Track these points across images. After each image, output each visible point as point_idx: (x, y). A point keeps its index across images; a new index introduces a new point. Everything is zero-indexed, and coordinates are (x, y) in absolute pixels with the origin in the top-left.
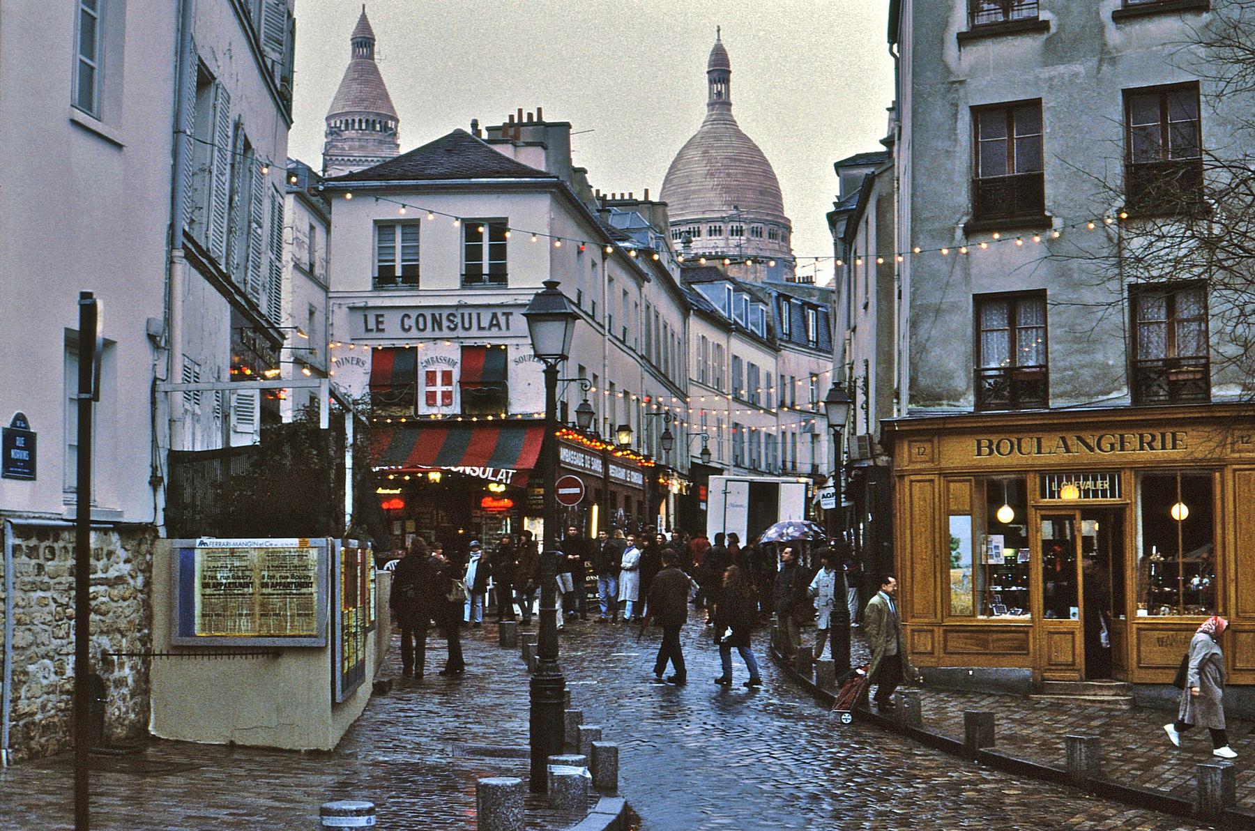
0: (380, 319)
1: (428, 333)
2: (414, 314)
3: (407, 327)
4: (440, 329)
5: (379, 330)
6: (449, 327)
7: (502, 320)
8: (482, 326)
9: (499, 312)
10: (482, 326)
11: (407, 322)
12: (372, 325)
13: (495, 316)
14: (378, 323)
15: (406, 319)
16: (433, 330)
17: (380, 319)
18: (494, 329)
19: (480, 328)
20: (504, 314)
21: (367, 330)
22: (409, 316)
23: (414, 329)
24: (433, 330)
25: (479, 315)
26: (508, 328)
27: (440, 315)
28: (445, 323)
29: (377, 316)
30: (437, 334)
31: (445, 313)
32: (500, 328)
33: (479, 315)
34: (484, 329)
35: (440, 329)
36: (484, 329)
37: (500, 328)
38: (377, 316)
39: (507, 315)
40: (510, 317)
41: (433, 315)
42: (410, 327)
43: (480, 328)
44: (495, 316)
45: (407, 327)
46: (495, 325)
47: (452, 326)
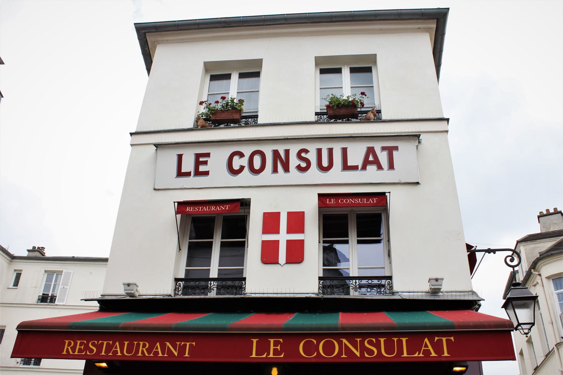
0: (201, 159)
1: (267, 176)
2: (247, 151)
3: (236, 167)
4: (286, 169)
5: (198, 173)
6: (299, 168)
7: (383, 157)
8: (349, 164)
9: (377, 146)
10: (349, 164)
11: (237, 163)
12: (188, 165)
13: (371, 150)
14: (198, 163)
15: (236, 158)
16: (275, 170)
17: (201, 159)
18: (372, 168)
19: (346, 167)
20: (384, 149)
21: (180, 174)
22: (241, 155)
23: (246, 169)
24: (275, 170)
25: (344, 151)
26: (391, 166)
27: (287, 152)
28: (294, 161)
29: (198, 156)
30: (281, 177)
31: (294, 149)
32: (380, 167)
33: (344, 151)
34: (355, 168)
35: (286, 169)
36: (355, 168)
37: (380, 167)
38: (198, 156)
39: (390, 150)
40: (395, 153)
41: (276, 154)
42: (242, 168)
43: (346, 167)
44: (371, 150)
45: (236, 167)
46: (371, 163)
47: (304, 165)
